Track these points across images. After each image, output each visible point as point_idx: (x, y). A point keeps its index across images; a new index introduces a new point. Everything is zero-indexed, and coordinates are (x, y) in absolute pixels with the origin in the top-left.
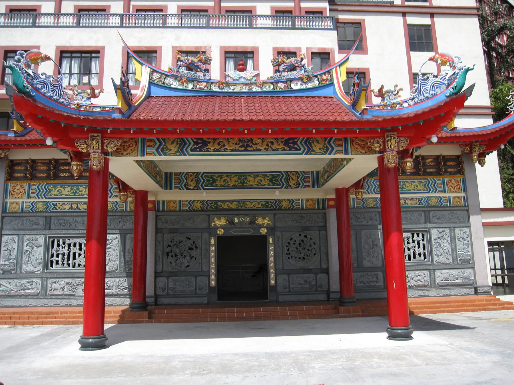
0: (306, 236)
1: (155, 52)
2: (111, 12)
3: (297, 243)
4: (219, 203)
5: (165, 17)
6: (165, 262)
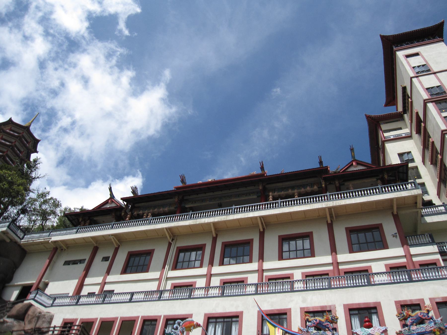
1: (286, 314)
2: (248, 283)
5: (292, 283)
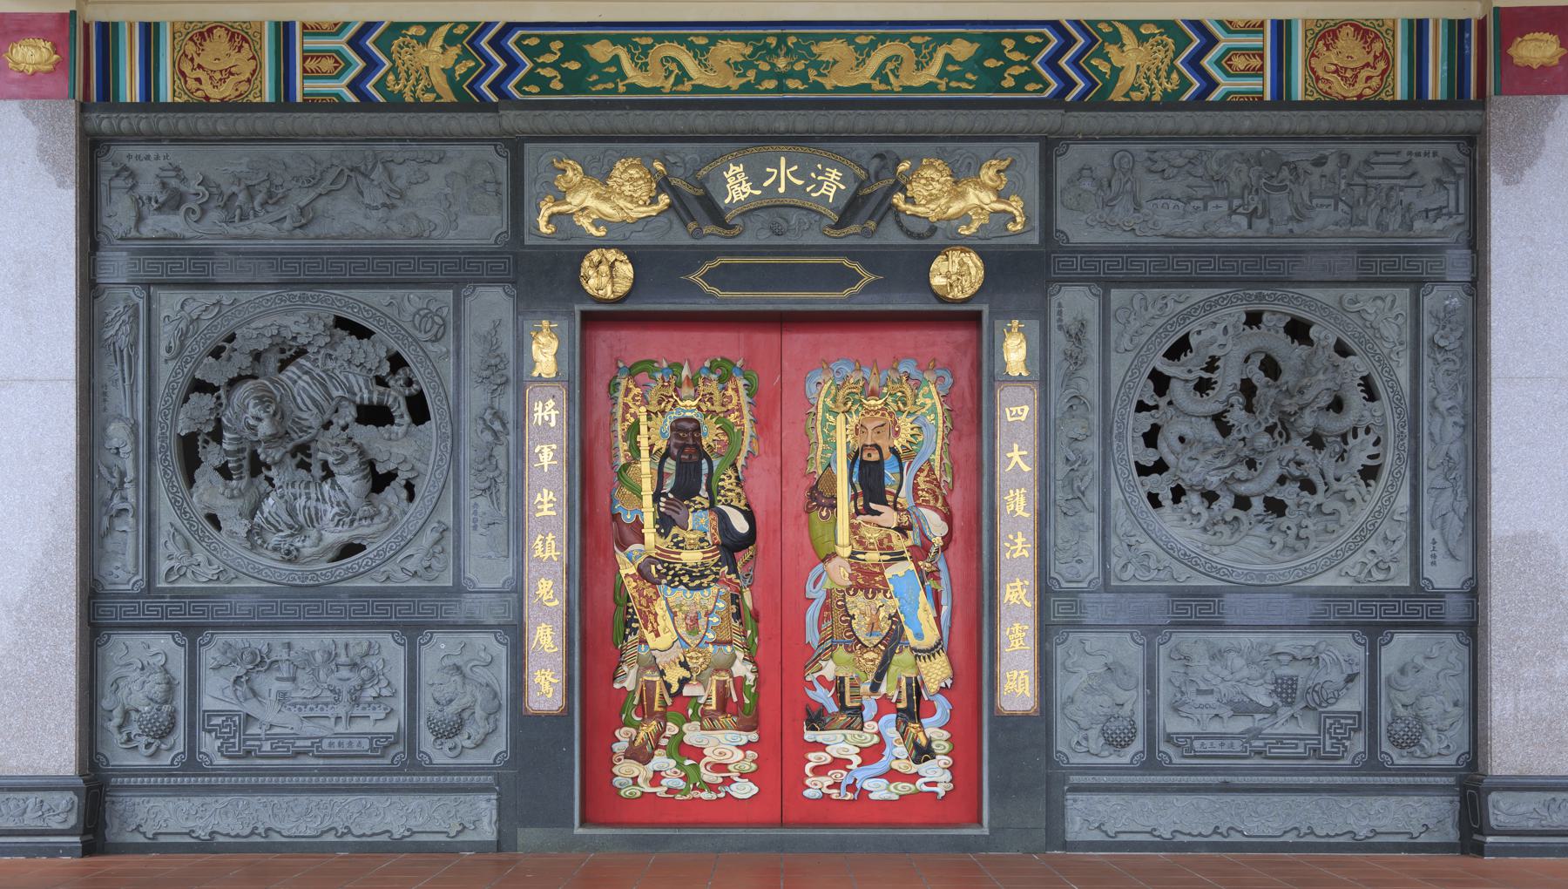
0: (1298, 330)
3: (1228, 379)
4: (601, 51)
6: (167, 515)
